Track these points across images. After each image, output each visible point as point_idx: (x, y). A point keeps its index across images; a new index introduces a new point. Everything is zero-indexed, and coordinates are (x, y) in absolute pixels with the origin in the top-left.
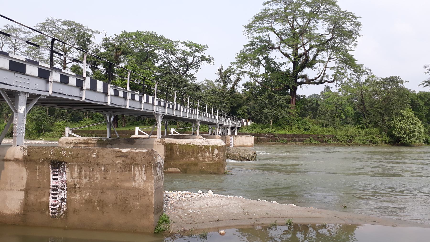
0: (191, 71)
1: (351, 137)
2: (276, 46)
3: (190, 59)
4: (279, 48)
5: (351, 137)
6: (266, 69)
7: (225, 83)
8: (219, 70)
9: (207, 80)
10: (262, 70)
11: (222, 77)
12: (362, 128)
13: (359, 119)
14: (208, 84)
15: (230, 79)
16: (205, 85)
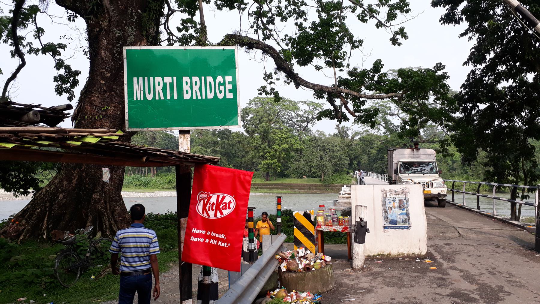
0: (310, 125)
1: (459, 186)
2: (396, 113)
3: (310, 116)
4: (398, 114)
5: (459, 186)
6: (385, 128)
7: (343, 137)
8: (337, 126)
9: (318, 131)
10: (382, 130)
11: (339, 132)
12: (467, 179)
13: (466, 168)
14: (319, 135)
15: (347, 133)
16: (317, 135)
